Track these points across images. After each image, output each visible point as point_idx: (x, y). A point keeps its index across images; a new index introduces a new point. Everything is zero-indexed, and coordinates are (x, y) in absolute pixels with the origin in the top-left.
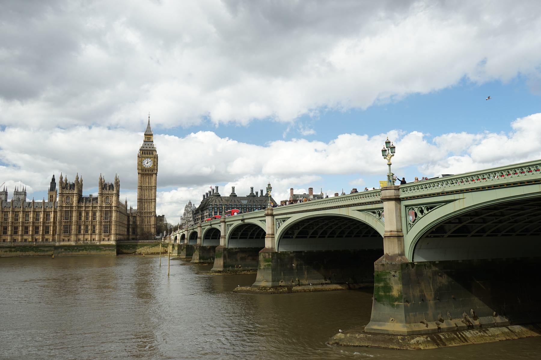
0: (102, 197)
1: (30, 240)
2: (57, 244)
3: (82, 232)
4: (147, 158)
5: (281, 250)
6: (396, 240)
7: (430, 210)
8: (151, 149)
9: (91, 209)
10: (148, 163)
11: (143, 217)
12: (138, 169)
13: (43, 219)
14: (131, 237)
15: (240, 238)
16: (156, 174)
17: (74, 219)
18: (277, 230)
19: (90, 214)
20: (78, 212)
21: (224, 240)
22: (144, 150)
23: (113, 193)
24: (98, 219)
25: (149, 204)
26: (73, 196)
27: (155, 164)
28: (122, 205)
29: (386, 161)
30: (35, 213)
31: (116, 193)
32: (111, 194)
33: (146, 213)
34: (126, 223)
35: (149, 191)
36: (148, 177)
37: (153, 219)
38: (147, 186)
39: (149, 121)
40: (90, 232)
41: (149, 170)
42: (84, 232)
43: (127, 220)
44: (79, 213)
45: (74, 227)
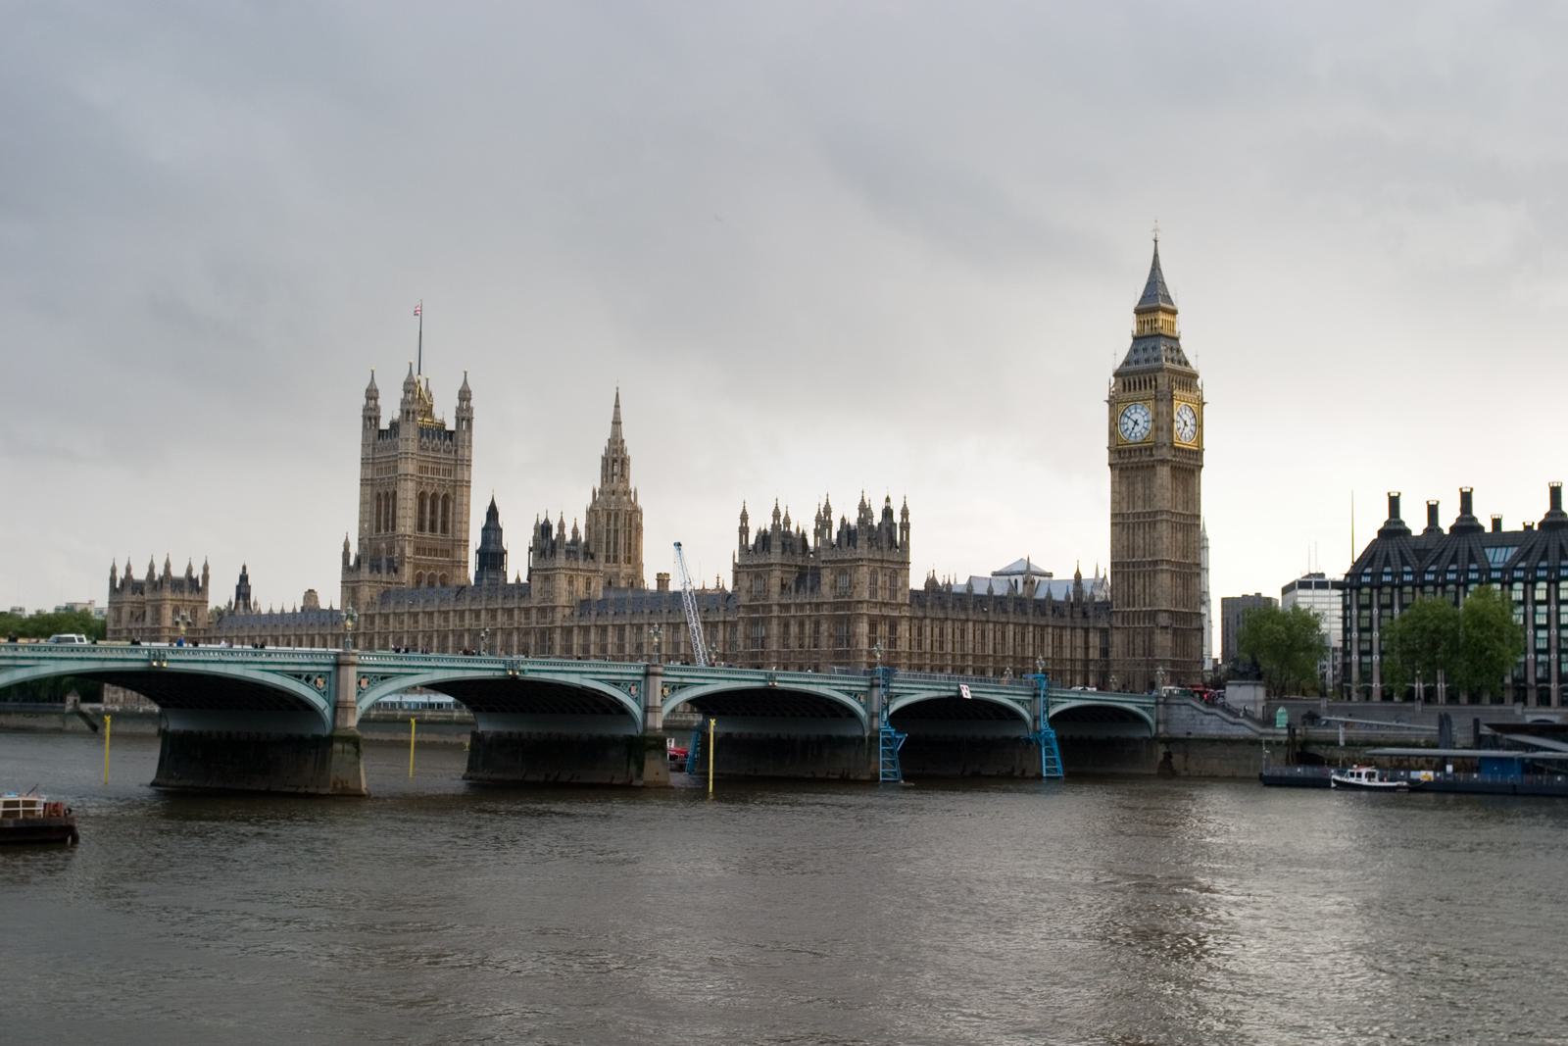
0: (829, 570)
10: (1139, 421)
11: (1131, 632)
12: (1108, 448)
19: (808, 628)
20: (779, 625)
23: (854, 557)
25: (1147, 579)
26: (769, 573)
30: (729, 629)
31: (858, 556)
32: (850, 561)
33: (1139, 619)
34: (1078, 656)
35: (1147, 529)
36: (1140, 478)
38: (1139, 513)
39: (1156, 255)
41: (1141, 451)
43: (1079, 641)
44: (782, 625)
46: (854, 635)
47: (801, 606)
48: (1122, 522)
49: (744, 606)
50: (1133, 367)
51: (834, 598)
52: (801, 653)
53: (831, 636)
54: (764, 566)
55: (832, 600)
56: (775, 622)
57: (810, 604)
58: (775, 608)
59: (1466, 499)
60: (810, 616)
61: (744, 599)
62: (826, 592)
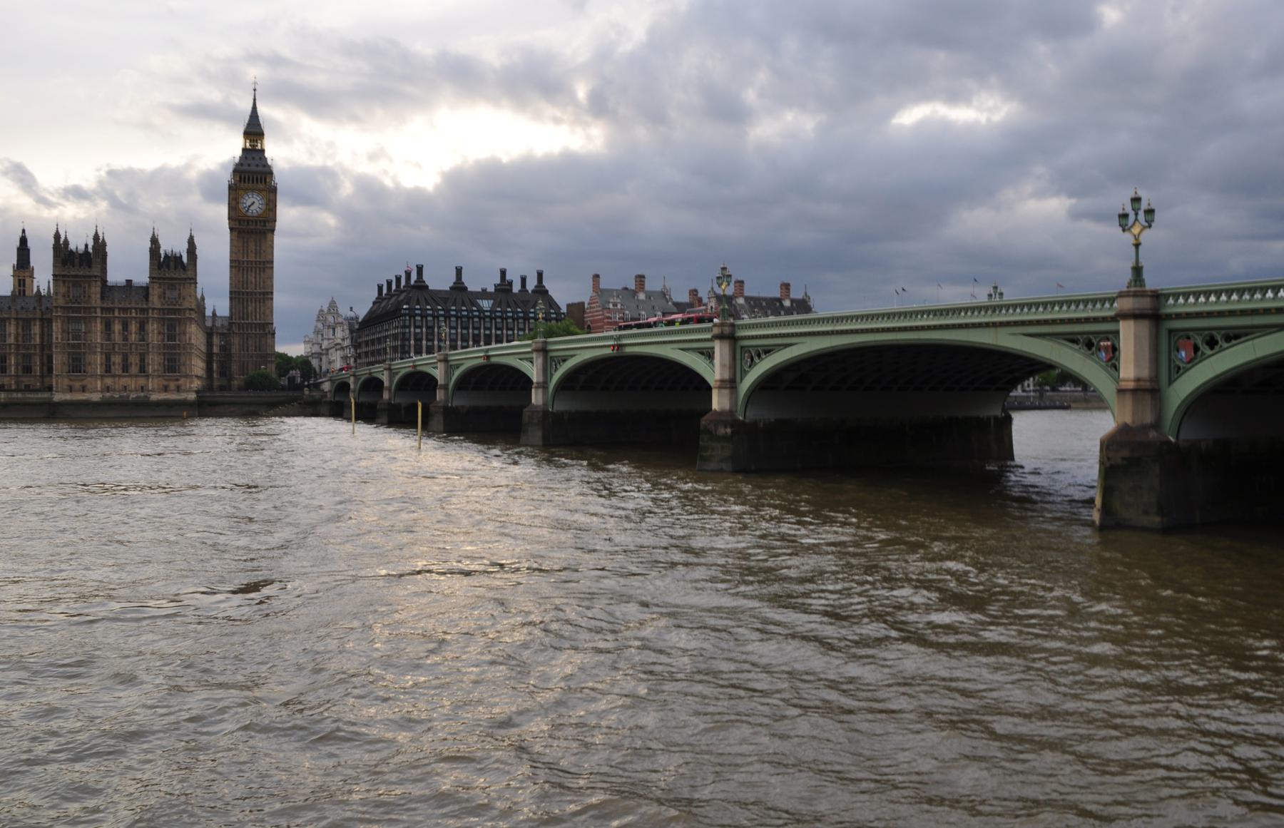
2: (58, 397)
4: (253, 190)
5: (751, 415)
6: (1148, 397)
7: (1234, 342)
8: (260, 169)
9: (134, 315)
10: (253, 203)
13: (17, 341)
16: (273, 231)
19: (133, 327)
22: (245, 172)
29: (1128, 238)
32: (180, 279)
39: (255, 100)
40: (134, 370)
46: (184, 333)
47: (125, 310)
48: (236, 265)
49: (61, 307)
51: (163, 304)
52: (124, 345)
53: (159, 333)
54: (84, 277)
55: (159, 306)
56: (99, 321)
57: (135, 309)
58: (99, 310)
59: (540, 275)
61: (61, 302)
62: (155, 301)
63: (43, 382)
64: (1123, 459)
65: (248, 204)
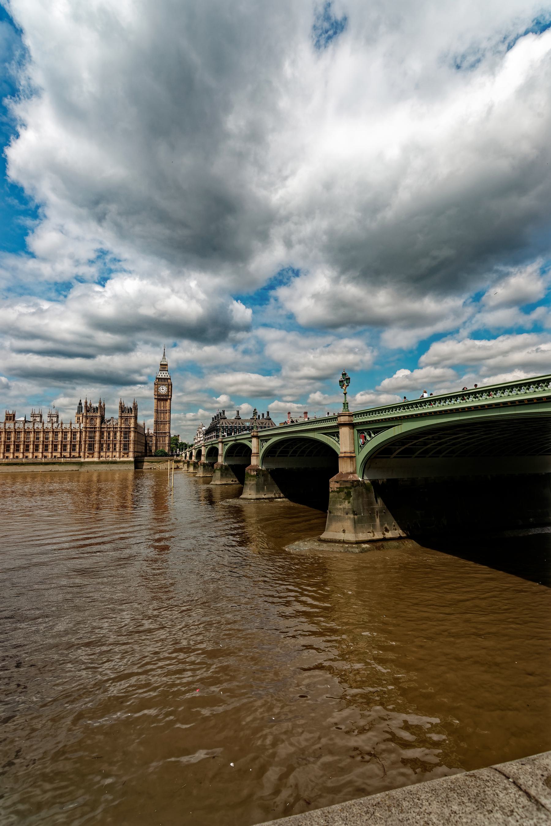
1: (59, 456)
3: (104, 450)
4: (163, 385)
10: (163, 390)
14: (148, 454)
15: (236, 456)
16: (170, 399)
17: (97, 438)
18: (261, 449)
21: (222, 458)
24: (118, 438)
27: (170, 390)
28: (140, 427)
37: (167, 438)
40: (111, 450)
42: (106, 450)
45: (97, 446)
47: (110, 428)
48: (157, 411)
50: (160, 377)
60: (113, 431)
63: (61, 455)
64: (337, 488)
65: (162, 390)
